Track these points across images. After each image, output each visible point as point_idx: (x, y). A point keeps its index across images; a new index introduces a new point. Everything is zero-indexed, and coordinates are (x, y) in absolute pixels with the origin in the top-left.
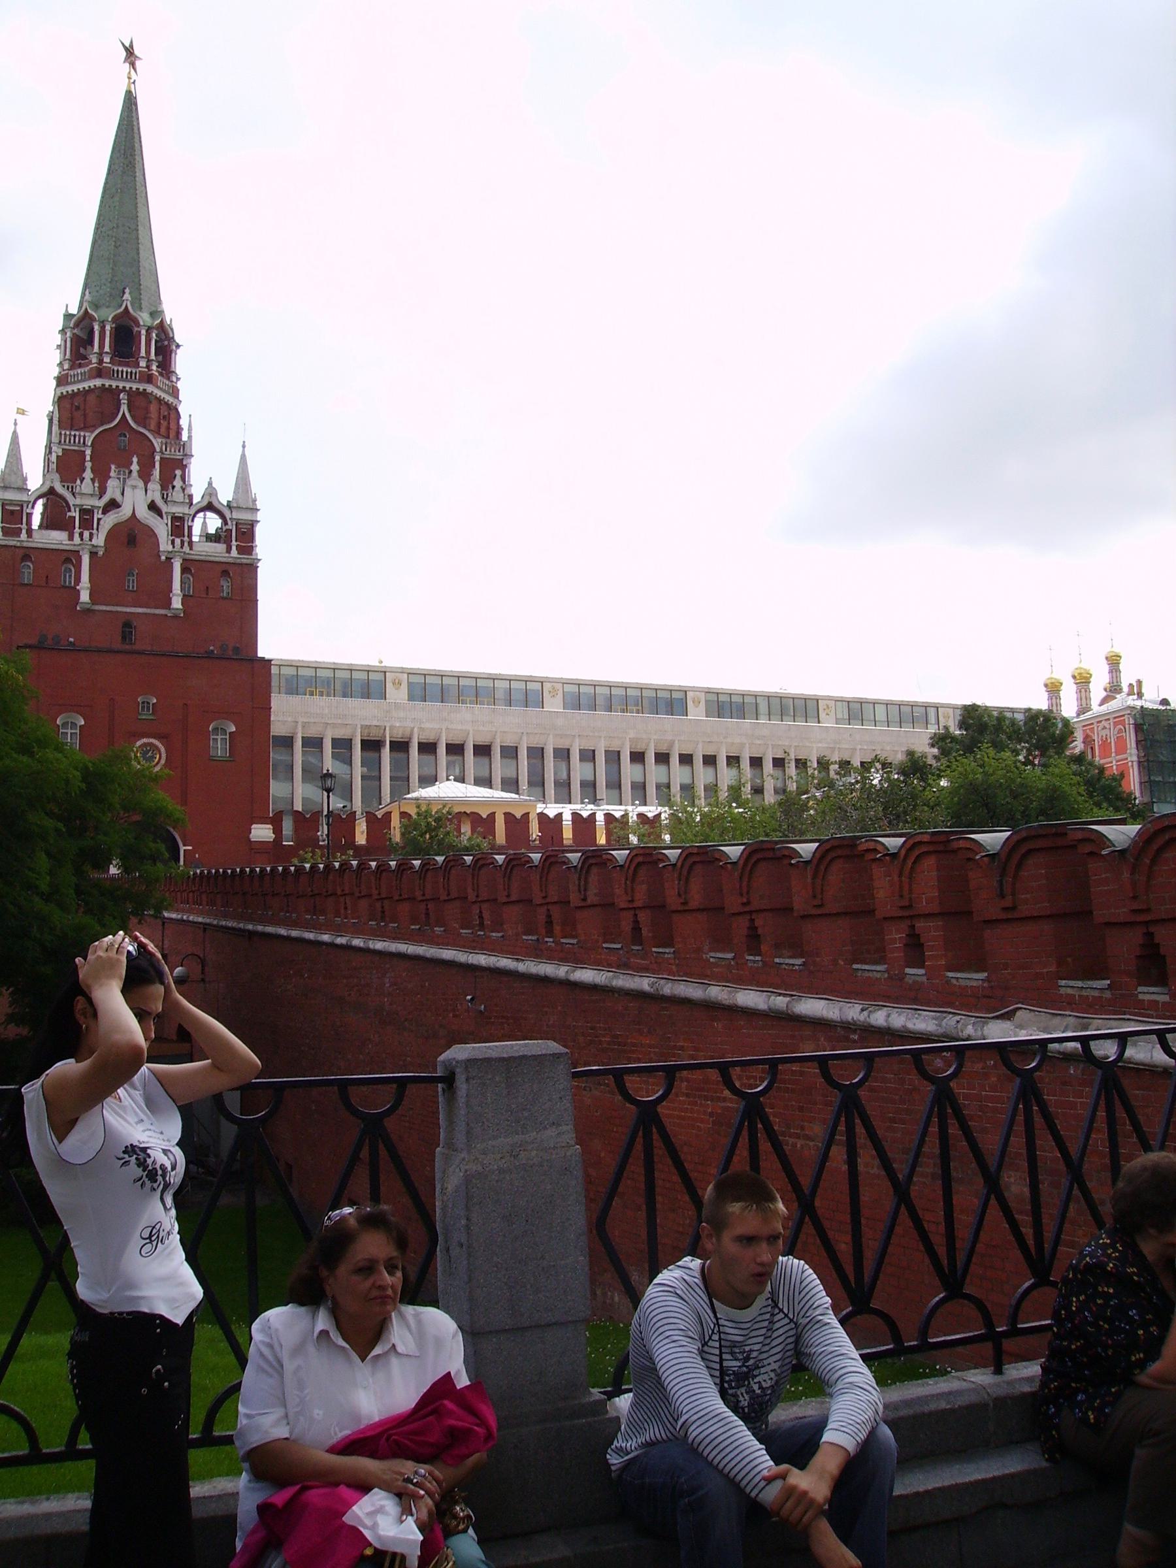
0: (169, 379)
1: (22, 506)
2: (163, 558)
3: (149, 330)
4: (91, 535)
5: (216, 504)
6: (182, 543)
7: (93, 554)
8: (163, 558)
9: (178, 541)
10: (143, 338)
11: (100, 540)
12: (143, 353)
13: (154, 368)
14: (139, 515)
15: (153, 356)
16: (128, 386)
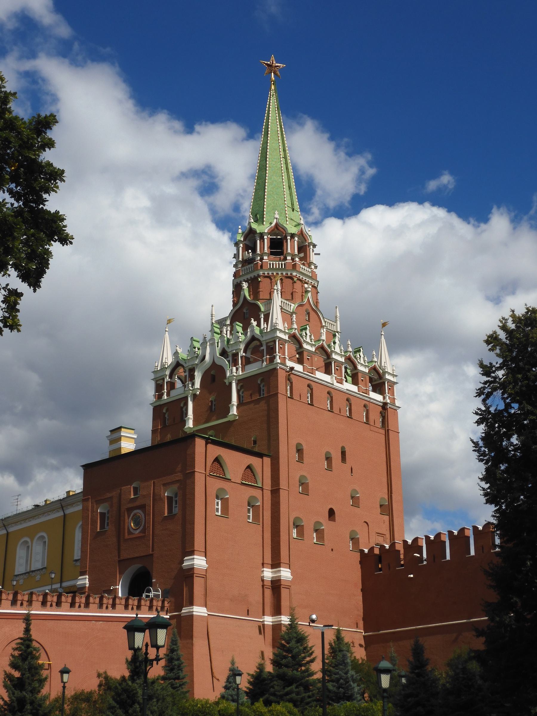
0: (285, 259)
1: (163, 379)
2: (227, 384)
3: (262, 236)
4: (193, 384)
5: (256, 336)
6: (237, 369)
7: (195, 396)
8: (227, 384)
9: (234, 368)
10: (258, 241)
11: (197, 385)
12: (258, 251)
13: (265, 258)
14: (216, 361)
15: (266, 250)
16: (248, 276)
